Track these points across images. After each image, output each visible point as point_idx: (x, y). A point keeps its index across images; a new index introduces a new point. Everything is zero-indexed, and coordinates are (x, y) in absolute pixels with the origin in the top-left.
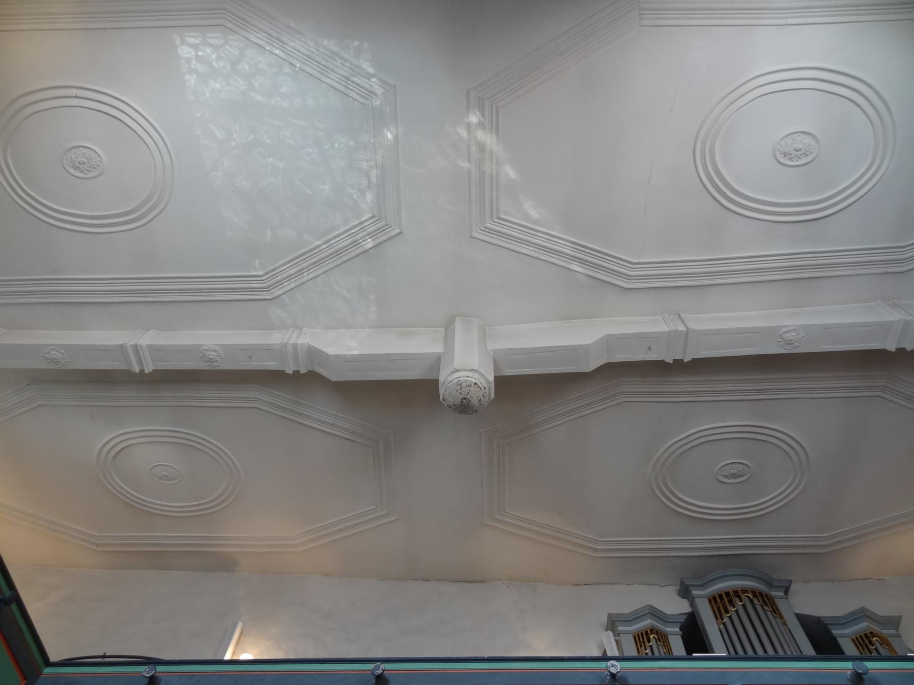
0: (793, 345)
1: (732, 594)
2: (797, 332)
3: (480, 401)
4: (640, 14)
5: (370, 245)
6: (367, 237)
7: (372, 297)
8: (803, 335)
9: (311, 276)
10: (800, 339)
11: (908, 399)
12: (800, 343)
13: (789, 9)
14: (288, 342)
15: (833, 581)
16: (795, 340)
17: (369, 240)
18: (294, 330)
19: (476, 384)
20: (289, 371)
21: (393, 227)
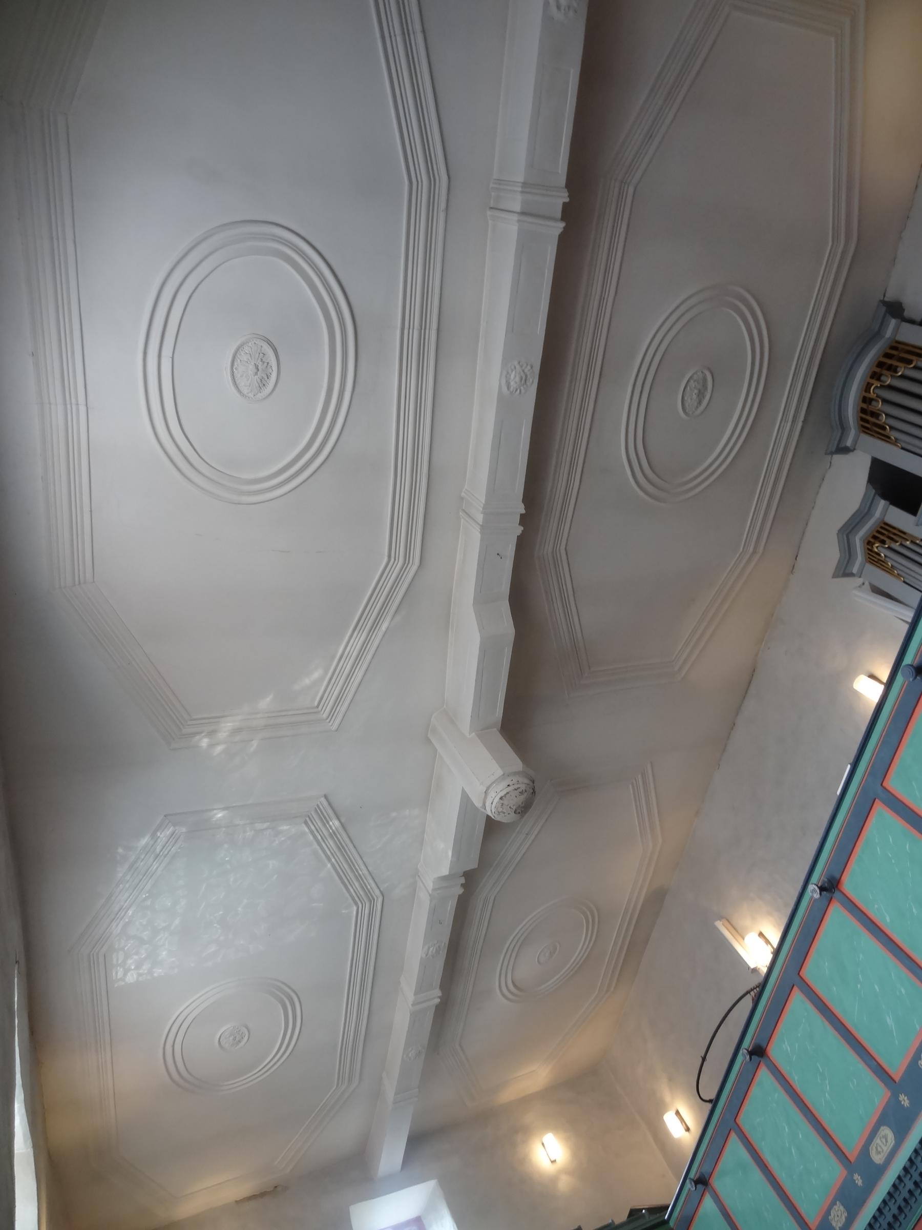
0: (528, 373)
1: (865, 406)
2: (510, 371)
3: (521, 793)
4: (80, 583)
5: (337, 823)
6: (328, 826)
7: (394, 814)
8: (516, 363)
9: (363, 867)
10: (521, 367)
11: (651, 136)
12: (527, 365)
13: (65, 404)
14: (430, 895)
15: (908, 217)
16: (522, 373)
17: (331, 823)
18: (419, 876)
19: (501, 798)
20: (460, 891)
21: (319, 803)
